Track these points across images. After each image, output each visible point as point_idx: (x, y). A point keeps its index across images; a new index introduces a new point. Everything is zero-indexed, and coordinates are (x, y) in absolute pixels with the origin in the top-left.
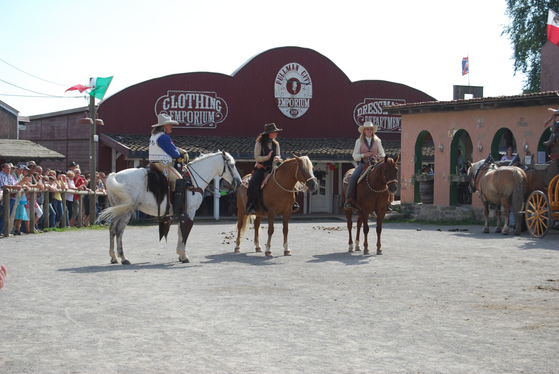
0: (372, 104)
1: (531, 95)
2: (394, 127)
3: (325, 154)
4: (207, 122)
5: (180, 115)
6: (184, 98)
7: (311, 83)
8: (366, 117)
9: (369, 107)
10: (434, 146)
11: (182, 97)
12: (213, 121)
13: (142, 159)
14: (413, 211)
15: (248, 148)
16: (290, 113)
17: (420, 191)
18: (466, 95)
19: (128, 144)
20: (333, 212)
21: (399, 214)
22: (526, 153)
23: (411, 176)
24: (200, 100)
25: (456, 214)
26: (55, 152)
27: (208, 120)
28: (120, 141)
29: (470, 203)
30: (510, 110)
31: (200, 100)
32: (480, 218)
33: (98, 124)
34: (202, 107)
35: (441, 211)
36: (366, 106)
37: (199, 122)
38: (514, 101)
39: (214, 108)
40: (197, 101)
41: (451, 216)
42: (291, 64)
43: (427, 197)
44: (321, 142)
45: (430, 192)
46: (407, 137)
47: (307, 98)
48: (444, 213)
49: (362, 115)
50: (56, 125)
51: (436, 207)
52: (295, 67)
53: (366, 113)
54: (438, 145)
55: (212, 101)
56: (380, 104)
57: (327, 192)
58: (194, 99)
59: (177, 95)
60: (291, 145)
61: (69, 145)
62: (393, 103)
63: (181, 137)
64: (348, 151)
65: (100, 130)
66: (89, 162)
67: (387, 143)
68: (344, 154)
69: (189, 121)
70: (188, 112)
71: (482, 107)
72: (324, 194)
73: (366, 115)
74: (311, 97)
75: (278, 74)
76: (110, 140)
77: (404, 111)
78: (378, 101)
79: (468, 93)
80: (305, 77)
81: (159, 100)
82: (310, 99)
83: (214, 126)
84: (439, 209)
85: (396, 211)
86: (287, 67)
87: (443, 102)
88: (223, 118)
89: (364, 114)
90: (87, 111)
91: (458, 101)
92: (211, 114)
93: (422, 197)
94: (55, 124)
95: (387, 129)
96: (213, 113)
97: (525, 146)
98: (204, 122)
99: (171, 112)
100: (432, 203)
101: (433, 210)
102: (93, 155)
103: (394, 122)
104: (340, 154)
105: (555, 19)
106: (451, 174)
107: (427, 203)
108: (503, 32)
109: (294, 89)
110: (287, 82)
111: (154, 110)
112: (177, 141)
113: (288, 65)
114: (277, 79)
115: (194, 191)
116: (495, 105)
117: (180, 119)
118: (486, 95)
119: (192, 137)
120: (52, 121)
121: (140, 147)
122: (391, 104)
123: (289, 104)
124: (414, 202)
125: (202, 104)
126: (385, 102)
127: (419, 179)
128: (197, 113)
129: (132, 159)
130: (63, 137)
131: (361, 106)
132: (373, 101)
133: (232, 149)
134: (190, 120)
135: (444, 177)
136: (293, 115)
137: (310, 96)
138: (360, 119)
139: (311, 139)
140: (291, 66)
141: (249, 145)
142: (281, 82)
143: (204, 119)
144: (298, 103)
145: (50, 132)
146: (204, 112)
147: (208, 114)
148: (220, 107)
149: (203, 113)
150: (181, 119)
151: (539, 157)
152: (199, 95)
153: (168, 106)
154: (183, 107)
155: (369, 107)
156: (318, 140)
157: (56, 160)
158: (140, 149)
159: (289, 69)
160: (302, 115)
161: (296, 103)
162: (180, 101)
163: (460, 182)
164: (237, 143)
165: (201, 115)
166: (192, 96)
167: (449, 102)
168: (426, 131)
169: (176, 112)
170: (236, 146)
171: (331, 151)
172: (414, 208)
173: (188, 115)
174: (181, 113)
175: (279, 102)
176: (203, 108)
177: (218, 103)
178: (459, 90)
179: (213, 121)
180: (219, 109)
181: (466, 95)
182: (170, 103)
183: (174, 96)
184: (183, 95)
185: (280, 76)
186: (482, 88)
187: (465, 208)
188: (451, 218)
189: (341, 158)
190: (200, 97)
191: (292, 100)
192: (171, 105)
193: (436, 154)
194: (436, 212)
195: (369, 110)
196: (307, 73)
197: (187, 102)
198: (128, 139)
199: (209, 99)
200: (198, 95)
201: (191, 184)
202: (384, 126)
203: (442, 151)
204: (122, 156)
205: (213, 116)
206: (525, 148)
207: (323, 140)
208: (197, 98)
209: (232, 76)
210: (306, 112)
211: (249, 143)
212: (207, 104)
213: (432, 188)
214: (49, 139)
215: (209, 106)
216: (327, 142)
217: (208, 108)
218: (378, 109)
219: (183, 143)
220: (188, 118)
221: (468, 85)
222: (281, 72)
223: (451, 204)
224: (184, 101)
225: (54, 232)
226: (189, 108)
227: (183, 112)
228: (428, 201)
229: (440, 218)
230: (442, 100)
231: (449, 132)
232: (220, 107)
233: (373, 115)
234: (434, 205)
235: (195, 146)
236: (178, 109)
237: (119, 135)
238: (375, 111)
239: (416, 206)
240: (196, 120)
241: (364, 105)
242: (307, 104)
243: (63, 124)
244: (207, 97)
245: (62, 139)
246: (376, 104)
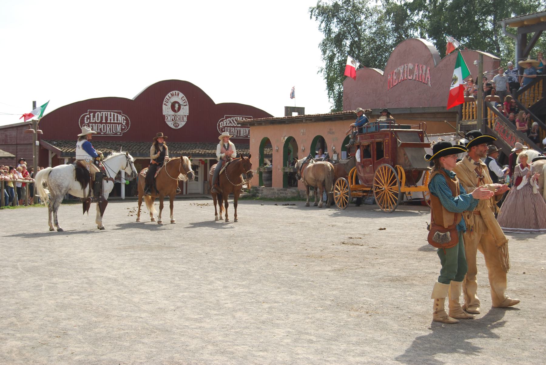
0: (230, 119)
1: (337, 113)
2: (245, 135)
3: (198, 153)
4: (116, 131)
5: (97, 127)
6: (99, 115)
7: (188, 105)
8: (226, 128)
9: (228, 121)
10: (272, 147)
11: (98, 114)
12: (120, 131)
13: (70, 158)
14: (258, 192)
15: (145, 150)
16: (174, 125)
17: (263, 178)
18: (293, 113)
19: (60, 147)
20: (204, 193)
21: (249, 194)
22: (333, 152)
23: (257, 168)
24: (111, 116)
25: (287, 194)
26: (8, 153)
27: (116, 130)
28: (54, 145)
29: (297, 186)
30: (323, 123)
31: (111, 116)
32: (304, 196)
33: (39, 134)
34: (112, 121)
35: (277, 192)
36: (226, 120)
37: (110, 132)
38: (325, 117)
39: (121, 122)
40: (109, 117)
41: (284, 195)
42: (174, 92)
43: (268, 183)
44: (195, 145)
45: (270, 179)
46: (254, 141)
47: (186, 114)
48: (279, 193)
49: (223, 127)
50: (9, 134)
51: (273, 189)
52: (177, 93)
53: (226, 125)
54: (275, 147)
55: (119, 117)
56: (235, 119)
57: (200, 179)
58: (106, 116)
59: (95, 113)
60: (174, 147)
61: (18, 148)
62: (244, 118)
63: (98, 142)
64: (213, 151)
65: (40, 137)
66: (32, 160)
67: (240, 146)
68: (211, 153)
69: (103, 131)
70: (103, 125)
71: (304, 121)
72: (197, 181)
73: (226, 126)
74: (188, 115)
75: (165, 99)
76: (47, 144)
77: (252, 124)
78: (234, 117)
79: (294, 112)
80: (184, 100)
81: (81, 116)
82: (187, 116)
83: (121, 134)
84: (276, 191)
85: (247, 192)
86: (171, 94)
87: (278, 118)
88: (127, 129)
89: (224, 126)
90: (31, 124)
91: (288, 117)
92: (119, 126)
93: (264, 183)
94: (8, 133)
95: (240, 136)
96: (120, 125)
97: (333, 148)
98: (114, 131)
99: (90, 124)
100: (271, 186)
101: (272, 191)
102: (35, 155)
103: (245, 131)
104: (208, 153)
105: (352, 62)
106: (283, 166)
107: (268, 186)
108: (318, 72)
109: (176, 109)
110: (171, 104)
111: (78, 124)
112: (95, 145)
113: (172, 92)
114: (164, 102)
115: (107, 180)
116: (313, 120)
117: (97, 129)
118: (307, 113)
119: (105, 142)
120: (6, 131)
121: (69, 149)
122: (242, 119)
123: (172, 119)
124: (259, 185)
125: (112, 119)
126: (238, 118)
127: (262, 170)
128: (109, 125)
129: (63, 158)
130: (14, 142)
131: (222, 121)
132: (231, 117)
133: (134, 150)
134: (104, 130)
135: (279, 169)
136: (175, 126)
138: (222, 129)
139: (188, 143)
140: (174, 93)
141: (145, 148)
142: (167, 104)
143: (114, 129)
144: (179, 119)
145: (4, 139)
146: (114, 125)
147: (116, 126)
148: (125, 121)
149: (113, 126)
150: (98, 130)
151: (343, 154)
152: (110, 113)
153: (89, 120)
154: (99, 121)
155: (228, 121)
156: (193, 144)
157: (9, 159)
158: (69, 150)
159: (172, 95)
160: (181, 126)
161: (178, 119)
162: (96, 117)
163: (290, 172)
164: (137, 146)
165: (111, 127)
166: (105, 114)
167: (282, 118)
168: (267, 138)
169: (94, 125)
170: (136, 148)
171: (202, 152)
172: (259, 190)
173: (102, 127)
174: (98, 125)
175: (166, 118)
176: (113, 122)
177: (124, 118)
178: (289, 110)
179: (120, 131)
180: (124, 122)
181: (293, 113)
182: (90, 118)
183: (93, 114)
184: (99, 113)
185: (166, 100)
186: (304, 108)
187: (293, 190)
188: (283, 196)
189: (209, 156)
190: (111, 114)
191: (175, 117)
192: (90, 120)
193: (274, 153)
194: (274, 192)
195: (228, 123)
196: (185, 98)
197: (102, 117)
198: (60, 144)
199: (117, 116)
200: (109, 113)
201: (106, 176)
202: (238, 134)
203: (277, 151)
204: (56, 156)
205: (120, 127)
206: (333, 149)
207: (196, 144)
208: (109, 115)
209: (133, 100)
210: (185, 124)
211: (145, 146)
212: (116, 119)
213: (271, 176)
214: (4, 144)
215: (117, 120)
216: (199, 145)
217: (116, 122)
218: (234, 123)
219: (99, 146)
220: (102, 129)
221: (294, 106)
222: (167, 97)
223: (284, 186)
224: (99, 117)
225: (8, 209)
226: (103, 122)
227: (99, 125)
228: (268, 185)
229: (277, 196)
230: (277, 117)
231: (282, 138)
232: (125, 121)
233: (230, 127)
234: (272, 188)
235: (107, 148)
236: (95, 123)
237: (54, 141)
238: (232, 124)
239: (260, 189)
240: (108, 130)
242: (185, 119)
243: (14, 133)
244: (116, 114)
245: (13, 143)
246: (232, 119)
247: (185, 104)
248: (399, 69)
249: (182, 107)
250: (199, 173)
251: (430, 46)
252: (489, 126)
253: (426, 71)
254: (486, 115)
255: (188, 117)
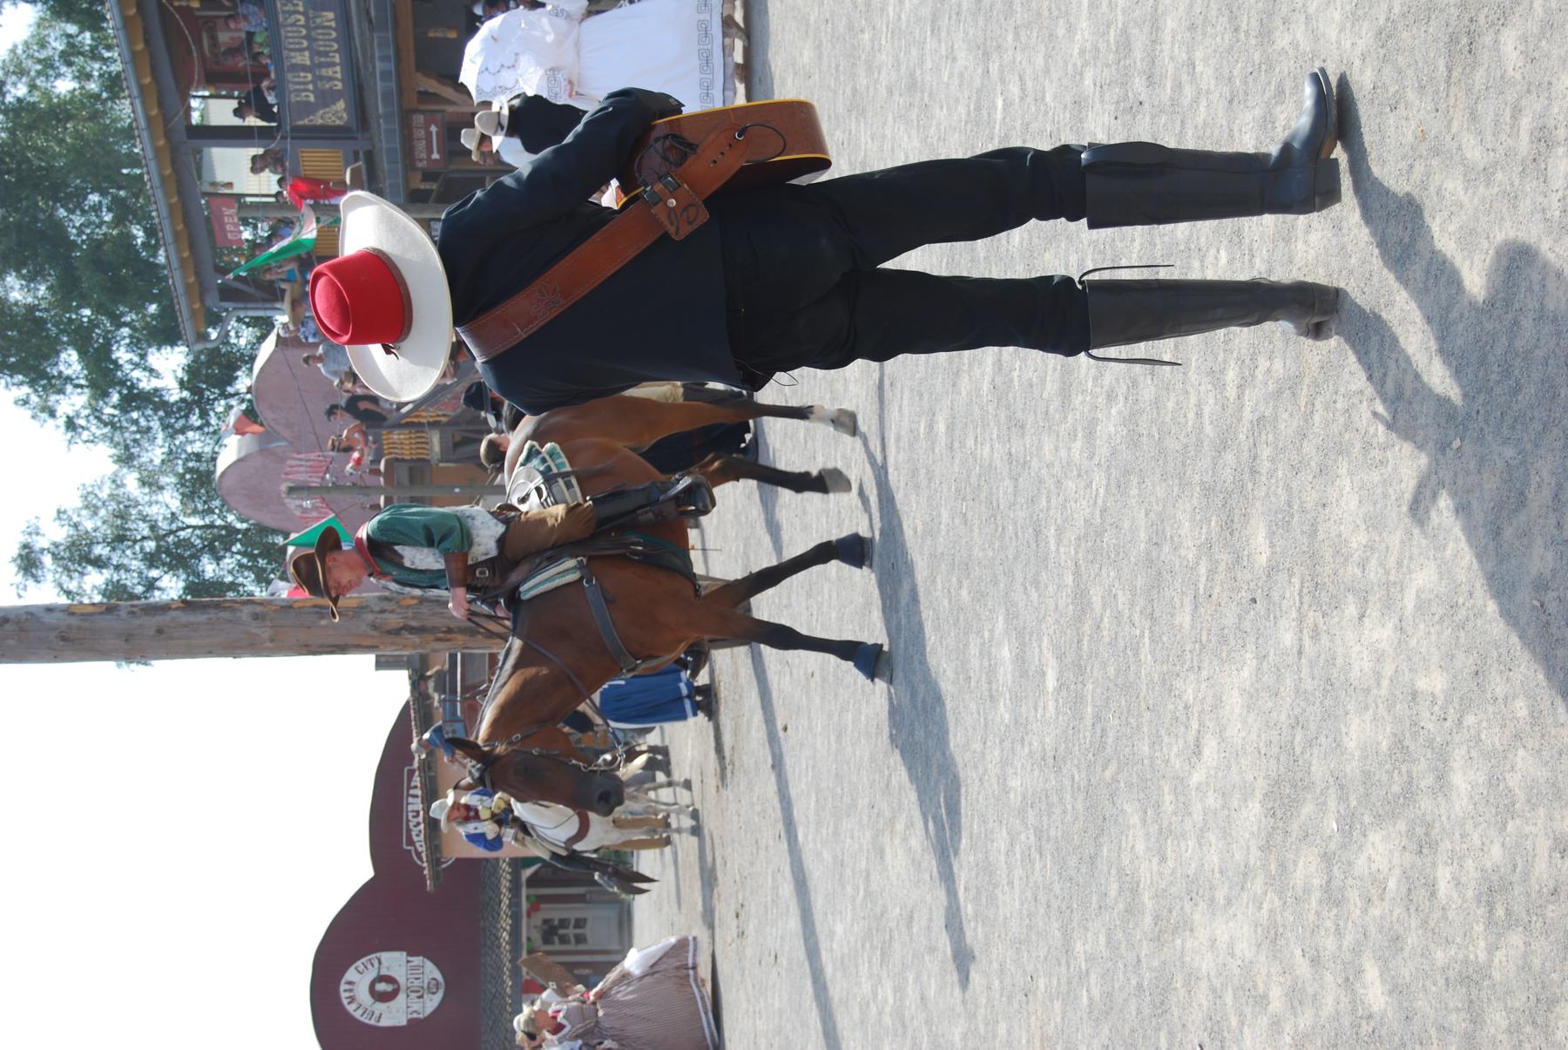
0: (414, 834)
3: (510, 935)
7: (378, 955)
36: (418, 845)
42: (344, 995)
52: (348, 987)
62: (411, 792)
72: (585, 920)
74: (404, 954)
78: (408, 821)
104: (509, 906)
109: (389, 988)
113: (345, 1002)
114: (372, 1022)
126: (410, 808)
132: (409, 831)
137: (400, 956)
140: (348, 994)
142: (377, 1014)
159: (352, 1000)
161: (417, 983)
171: (506, 923)
175: (415, 1016)
189: (518, 904)
196: (359, 963)
210: (432, 961)
222: (357, 1015)
241: (416, 850)
242: (417, 960)
247: (376, 963)
248: (293, 507)
249: (384, 972)
250: (564, 915)
251: (239, 452)
252: (444, 419)
253: (301, 460)
254: (420, 425)
255: (409, 954)
